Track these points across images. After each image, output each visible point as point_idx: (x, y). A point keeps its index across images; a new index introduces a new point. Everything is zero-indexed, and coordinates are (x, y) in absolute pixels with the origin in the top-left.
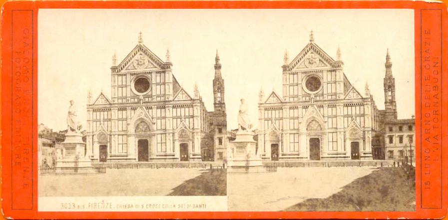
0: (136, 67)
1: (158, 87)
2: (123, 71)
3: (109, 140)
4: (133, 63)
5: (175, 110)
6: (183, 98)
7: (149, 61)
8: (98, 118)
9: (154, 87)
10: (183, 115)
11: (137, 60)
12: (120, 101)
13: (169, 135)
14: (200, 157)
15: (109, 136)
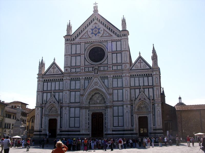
0: (91, 36)
1: (114, 55)
2: (77, 40)
3: (59, 113)
4: (87, 31)
5: (132, 79)
6: (141, 67)
7: (104, 29)
8: (49, 89)
9: (110, 55)
10: (141, 84)
11: (92, 30)
12: (73, 70)
13: (127, 106)
14: (162, 131)
15: (59, 109)
